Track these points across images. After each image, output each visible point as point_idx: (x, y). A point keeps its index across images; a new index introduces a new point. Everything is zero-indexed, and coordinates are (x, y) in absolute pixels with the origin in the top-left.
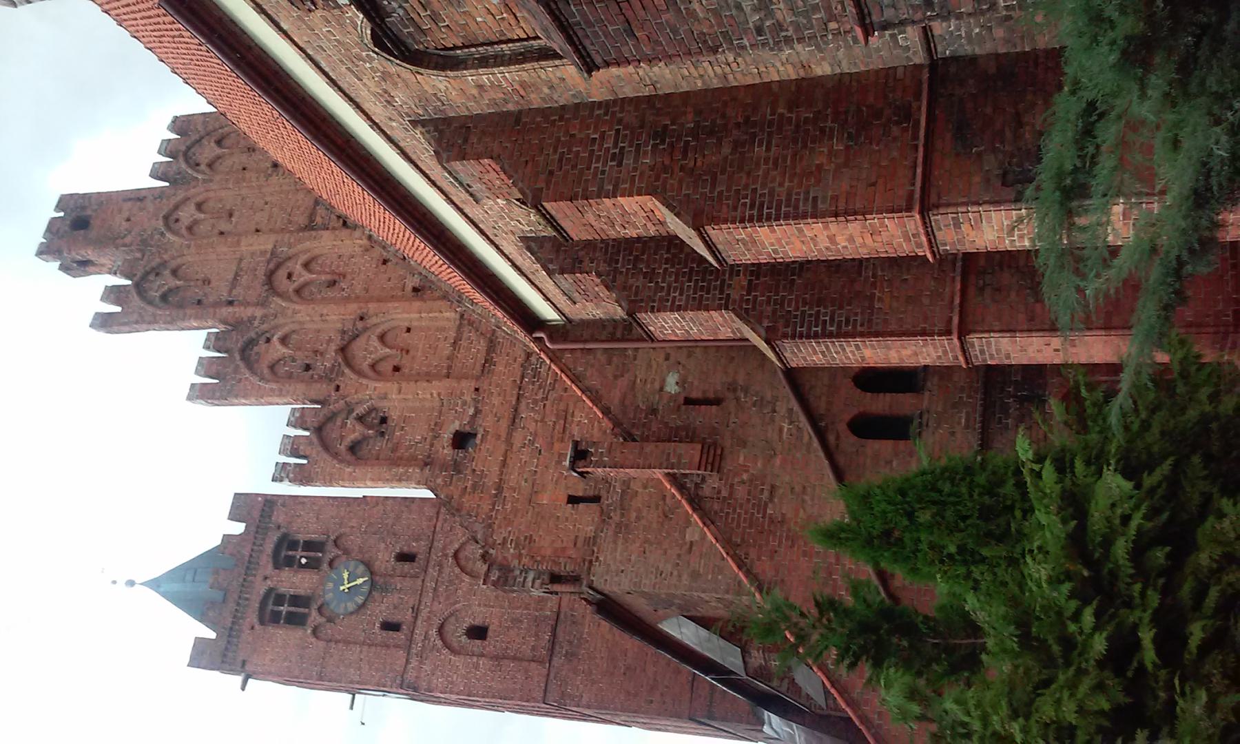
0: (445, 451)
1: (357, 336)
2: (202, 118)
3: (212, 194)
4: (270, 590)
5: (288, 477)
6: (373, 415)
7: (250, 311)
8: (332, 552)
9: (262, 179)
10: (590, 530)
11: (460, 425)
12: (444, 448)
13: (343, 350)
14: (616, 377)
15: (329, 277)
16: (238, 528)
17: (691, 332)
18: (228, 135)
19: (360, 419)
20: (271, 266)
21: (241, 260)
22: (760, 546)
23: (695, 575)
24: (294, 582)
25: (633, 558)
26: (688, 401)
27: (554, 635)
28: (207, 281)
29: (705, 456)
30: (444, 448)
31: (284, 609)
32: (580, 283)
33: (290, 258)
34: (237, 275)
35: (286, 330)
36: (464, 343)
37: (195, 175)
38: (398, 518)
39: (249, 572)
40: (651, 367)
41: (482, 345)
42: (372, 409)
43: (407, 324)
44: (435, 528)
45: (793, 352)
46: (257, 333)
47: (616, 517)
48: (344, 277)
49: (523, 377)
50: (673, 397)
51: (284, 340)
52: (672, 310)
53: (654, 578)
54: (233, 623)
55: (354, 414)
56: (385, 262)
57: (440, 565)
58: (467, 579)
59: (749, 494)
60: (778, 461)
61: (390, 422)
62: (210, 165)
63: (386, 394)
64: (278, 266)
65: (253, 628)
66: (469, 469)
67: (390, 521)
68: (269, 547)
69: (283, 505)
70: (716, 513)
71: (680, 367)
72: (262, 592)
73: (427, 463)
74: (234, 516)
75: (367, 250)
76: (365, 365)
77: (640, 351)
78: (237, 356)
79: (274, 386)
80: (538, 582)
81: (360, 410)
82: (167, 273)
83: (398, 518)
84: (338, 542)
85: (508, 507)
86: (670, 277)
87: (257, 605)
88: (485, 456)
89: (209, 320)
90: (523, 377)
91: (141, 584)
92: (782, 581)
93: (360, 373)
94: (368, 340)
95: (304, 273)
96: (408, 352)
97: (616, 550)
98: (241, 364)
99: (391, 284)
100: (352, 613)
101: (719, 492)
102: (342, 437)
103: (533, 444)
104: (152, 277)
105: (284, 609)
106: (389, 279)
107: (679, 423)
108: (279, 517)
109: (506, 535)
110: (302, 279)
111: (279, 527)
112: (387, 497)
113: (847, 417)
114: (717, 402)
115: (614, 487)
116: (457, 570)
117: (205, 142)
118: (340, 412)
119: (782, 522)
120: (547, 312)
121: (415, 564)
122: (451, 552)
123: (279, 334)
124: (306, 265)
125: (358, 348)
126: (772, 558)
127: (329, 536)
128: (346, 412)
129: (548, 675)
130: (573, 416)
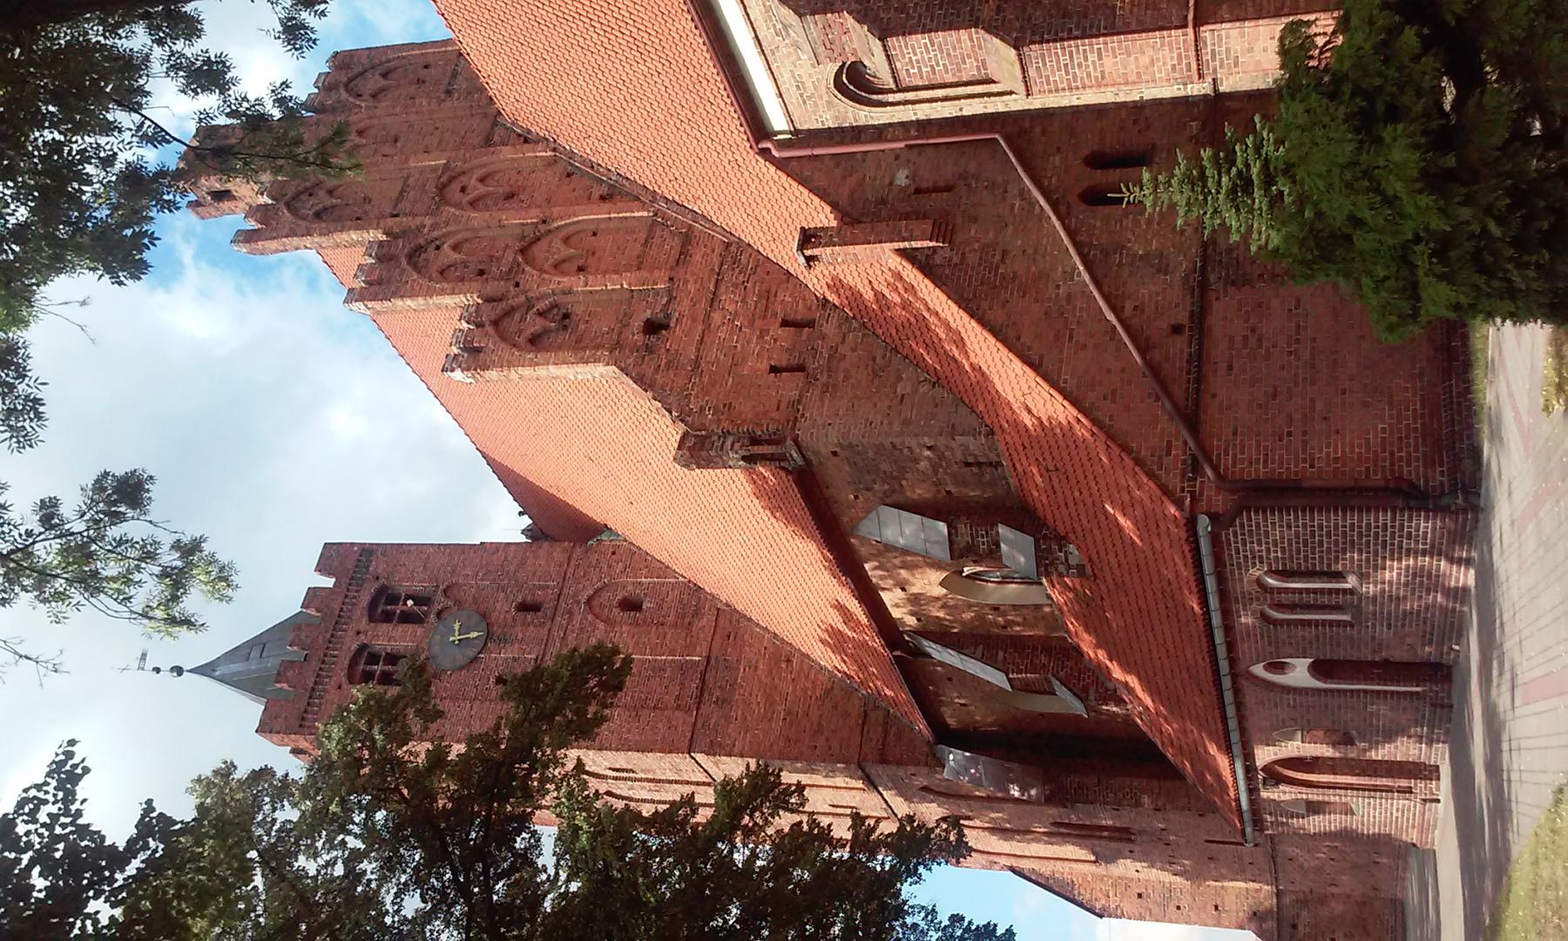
0: (636, 337)
1: (539, 239)
2: (367, 52)
3: (375, 122)
4: (363, 647)
5: (460, 367)
6: (555, 311)
7: (418, 220)
8: (440, 602)
9: (434, 105)
10: (795, 394)
11: (652, 313)
12: (634, 335)
13: (523, 251)
14: (844, 178)
15: (507, 189)
16: (329, 582)
17: (937, 69)
18: (395, 69)
19: (540, 314)
20: (443, 179)
21: (408, 177)
22: (992, 299)
23: (906, 422)
24: (394, 638)
25: (841, 412)
26: (918, 191)
27: (703, 681)
28: (367, 200)
29: (936, 230)
30: (634, 335)
31: (378, 669)
32: (827, 28)
33: (464, 173)
34: (403, 191)
35: (459, 237)
36: (657, 240)
37: (358, 103)
38: (522, 563)
39: (338, 627)
40: (881, 166)
41: (677, 241)
42: (555, 306)
43: (592, 227)
44: (565, 573)
45: (1038, 68)
46: (427, 240)
47: (824, 379)
48: (524, 189)
49: (722, 264)
50: (902, 189)
51: (455, 247)
52: (923, 33)
53: (863, 426)
54: (316, 683)
55: (535, 309)
56: (569, 175)
57: (571, 613)
58: (601, 626)
59: (980, 259)
60: (1010, 230)
61: (574, 318)
62: (374, 96)
63: (571, 288)
64: (452, 179)
65: (340, 687)
66: (663, 350)
67: (512, 568)
68: (365, 599)
69: (383, 554)
70: (947, 277)
71: (911, 165)
72: (354, 647)
73: (617, 346)
74: (323, 567)
75: (550, 165)
76: (547, 266)
77: (869, 154)
78: (404, 262)
79: (446, 286)
80: (737, 446)
81: (541, 306)
82: (322, 193)
83: (522, 563)
84: (448, 593)
85: (706, 379)
86: (921, 8)
87: (347, 662)
88: (681, 339)
89: (371, 231)
90: (722, 264)
91: (188, 671)
92: (1014, 323)
93: (542, 271)
94: (551, 242)
95: (479, 185)
96: (594, 253)
97: (823, 406)
98: (409, 268)
99: (575, 194)
100: (462, 668)
101: (951, 260)
102: (520, 331)
103: (733, 321)
104: (304, 197)
105: (378, 669)
106: (574, 190)
107: (909, 209)
108: (377, 566)
109: (704, 404)
110: (477, 192)
111: (378, 578)
112: (509, 544)
113: (1078, 190)
114: (949, 189)
115: (821, 353)
116: (590, 617)
117: (369, 75)
118: (519, 307)
119: (1014, 278)
120: (778, 121)
121: (540, 614)
122: (583, 598)
123: (451, 242)
124: (482, 180)
125: (539, 250)
126: (1003, 306)
127: (438, 586)
128: (525, 308)
129: (695, 724)
130: (776, 295)
